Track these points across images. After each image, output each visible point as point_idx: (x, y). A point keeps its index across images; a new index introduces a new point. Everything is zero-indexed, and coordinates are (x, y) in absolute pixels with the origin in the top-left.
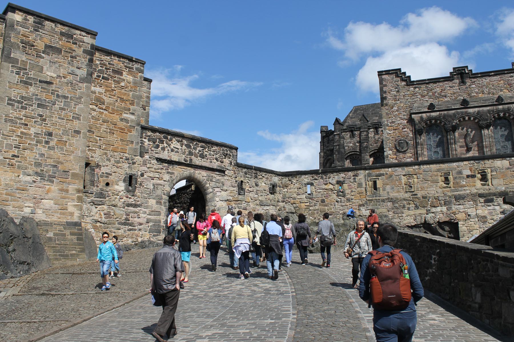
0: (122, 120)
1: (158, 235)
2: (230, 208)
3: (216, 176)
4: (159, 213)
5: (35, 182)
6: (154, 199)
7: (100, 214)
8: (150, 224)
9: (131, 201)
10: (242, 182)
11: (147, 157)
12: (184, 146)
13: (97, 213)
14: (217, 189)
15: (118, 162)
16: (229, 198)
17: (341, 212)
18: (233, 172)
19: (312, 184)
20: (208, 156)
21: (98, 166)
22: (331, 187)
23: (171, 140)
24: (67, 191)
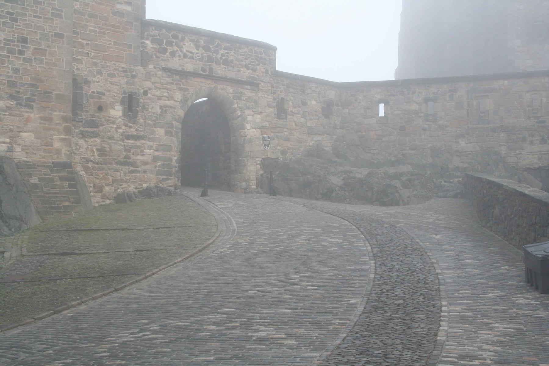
0: (115, 13)
1: (168, 179)
3: (248, 92)
5: (9, 108)
6: (161, 127)
7: (92, 151)
8: (159, 163)
9: (133, 131)
10: (283, 99)
11: (151, 67)
12: (201, 49)
13: (87, 148)
14: (247, 112)
15: (112, 75)
17: (429, 146)
19: (386, 103)
20: (235, 62)
21: (87, 82)
22: (415, 107)
23: (183, 40)
24: (50, 120)
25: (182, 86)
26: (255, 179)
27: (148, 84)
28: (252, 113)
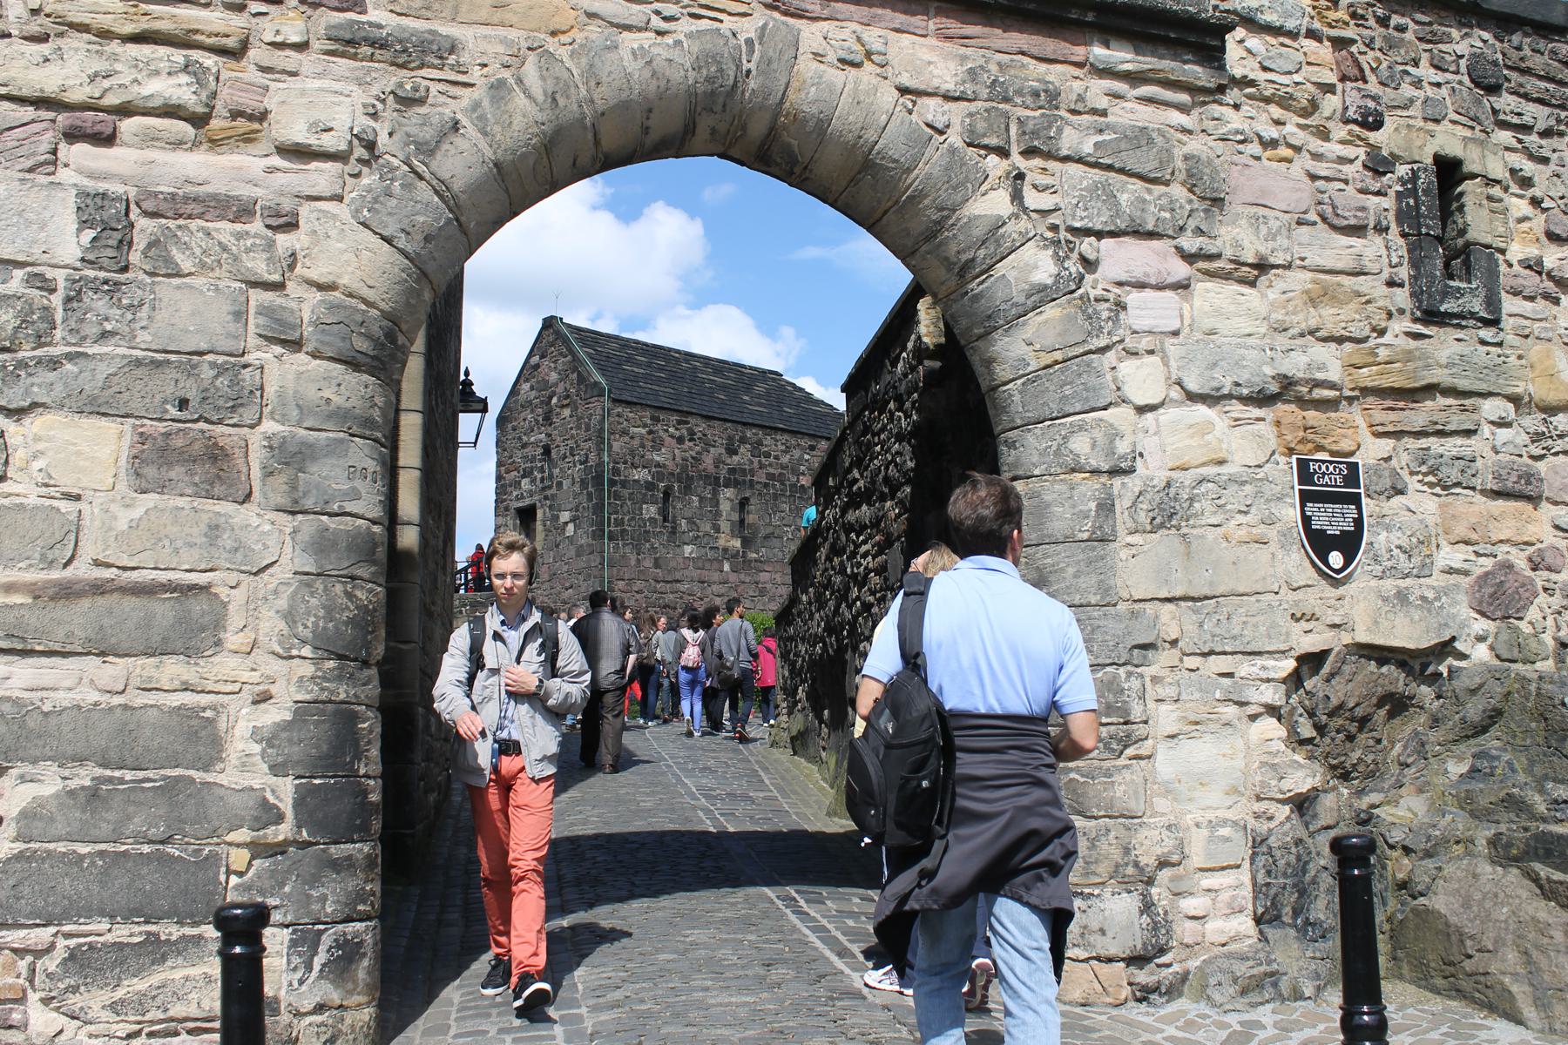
2: (1331, 480)
4: (183, 617)
6: (95, 407)
14: (1120, 259)
16: (1295, 364)
18: (1324, 51)
26: (1241, 850)
28: (1181, 270)
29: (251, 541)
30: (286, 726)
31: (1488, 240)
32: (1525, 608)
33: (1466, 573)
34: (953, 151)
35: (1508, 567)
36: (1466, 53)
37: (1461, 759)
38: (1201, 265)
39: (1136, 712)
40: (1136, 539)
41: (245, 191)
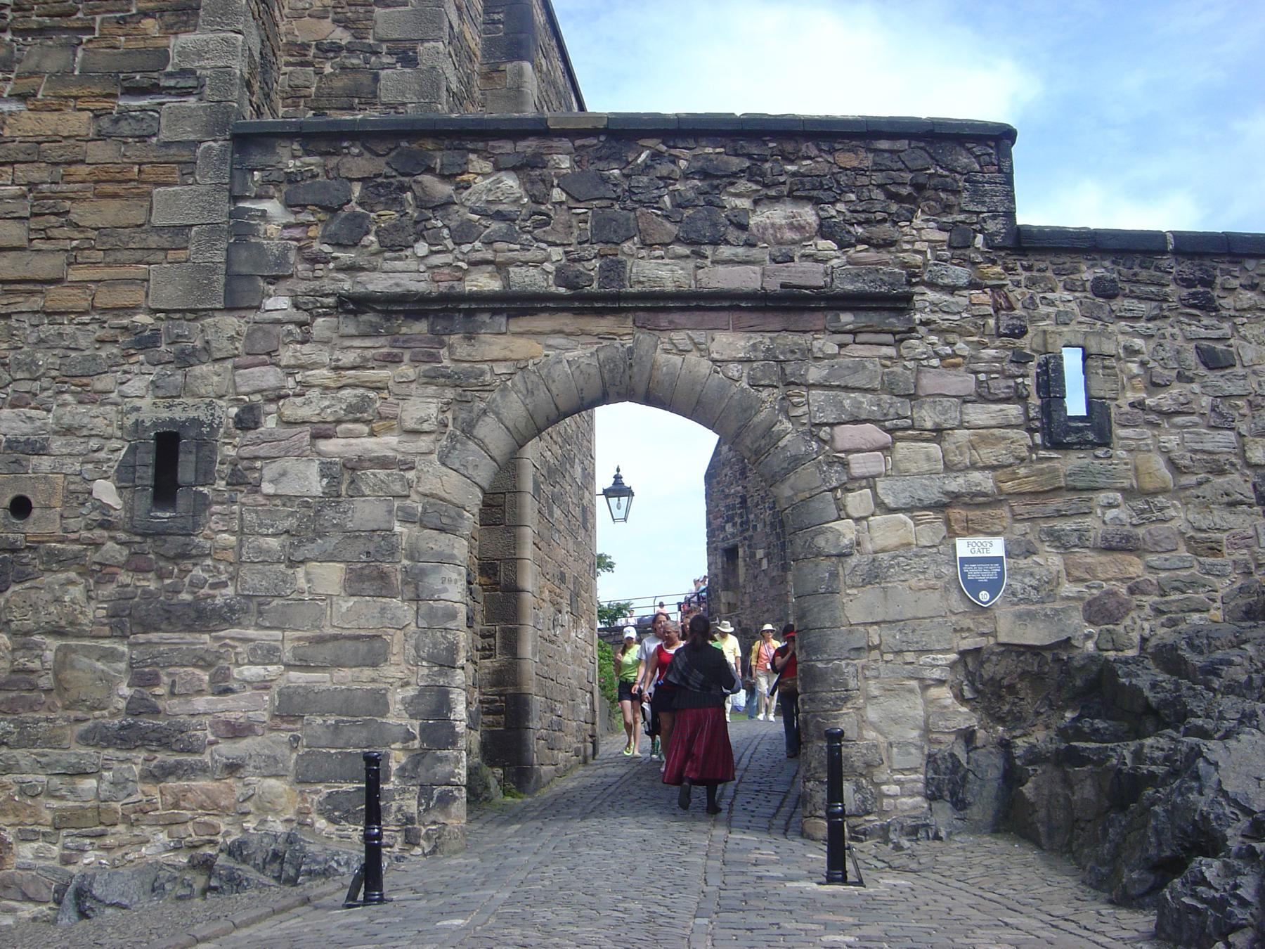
4: (371, 650)
14: (847, 435)
25: (446, 362)
27: (269, 377)
29: (399, 613)
30: (413, 698)
31: (1102, 394)
32: (1123, 617)
33: (1081, 599)
34: (743, 390)
35: (1113, 594)
36: (1091, 278)
37: (1074, 710)
38: (899, 434)
39: (852, 684)
40: (854, 591)
41: (390, 454)
